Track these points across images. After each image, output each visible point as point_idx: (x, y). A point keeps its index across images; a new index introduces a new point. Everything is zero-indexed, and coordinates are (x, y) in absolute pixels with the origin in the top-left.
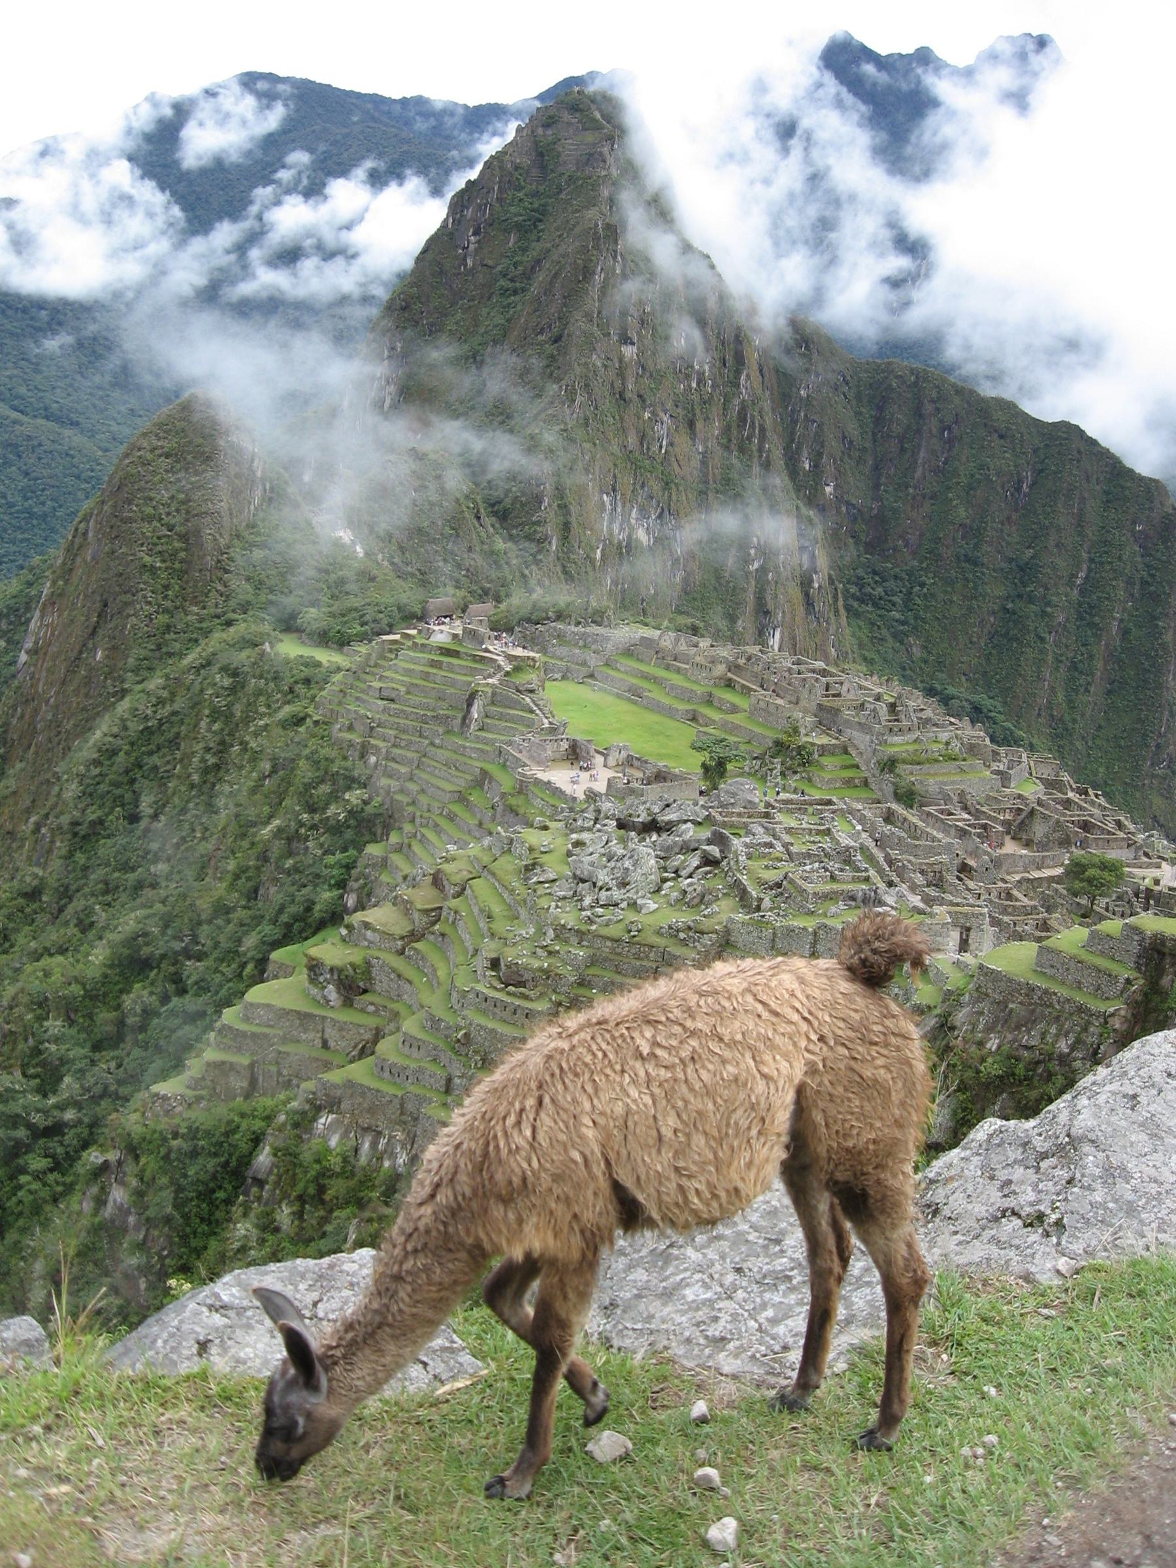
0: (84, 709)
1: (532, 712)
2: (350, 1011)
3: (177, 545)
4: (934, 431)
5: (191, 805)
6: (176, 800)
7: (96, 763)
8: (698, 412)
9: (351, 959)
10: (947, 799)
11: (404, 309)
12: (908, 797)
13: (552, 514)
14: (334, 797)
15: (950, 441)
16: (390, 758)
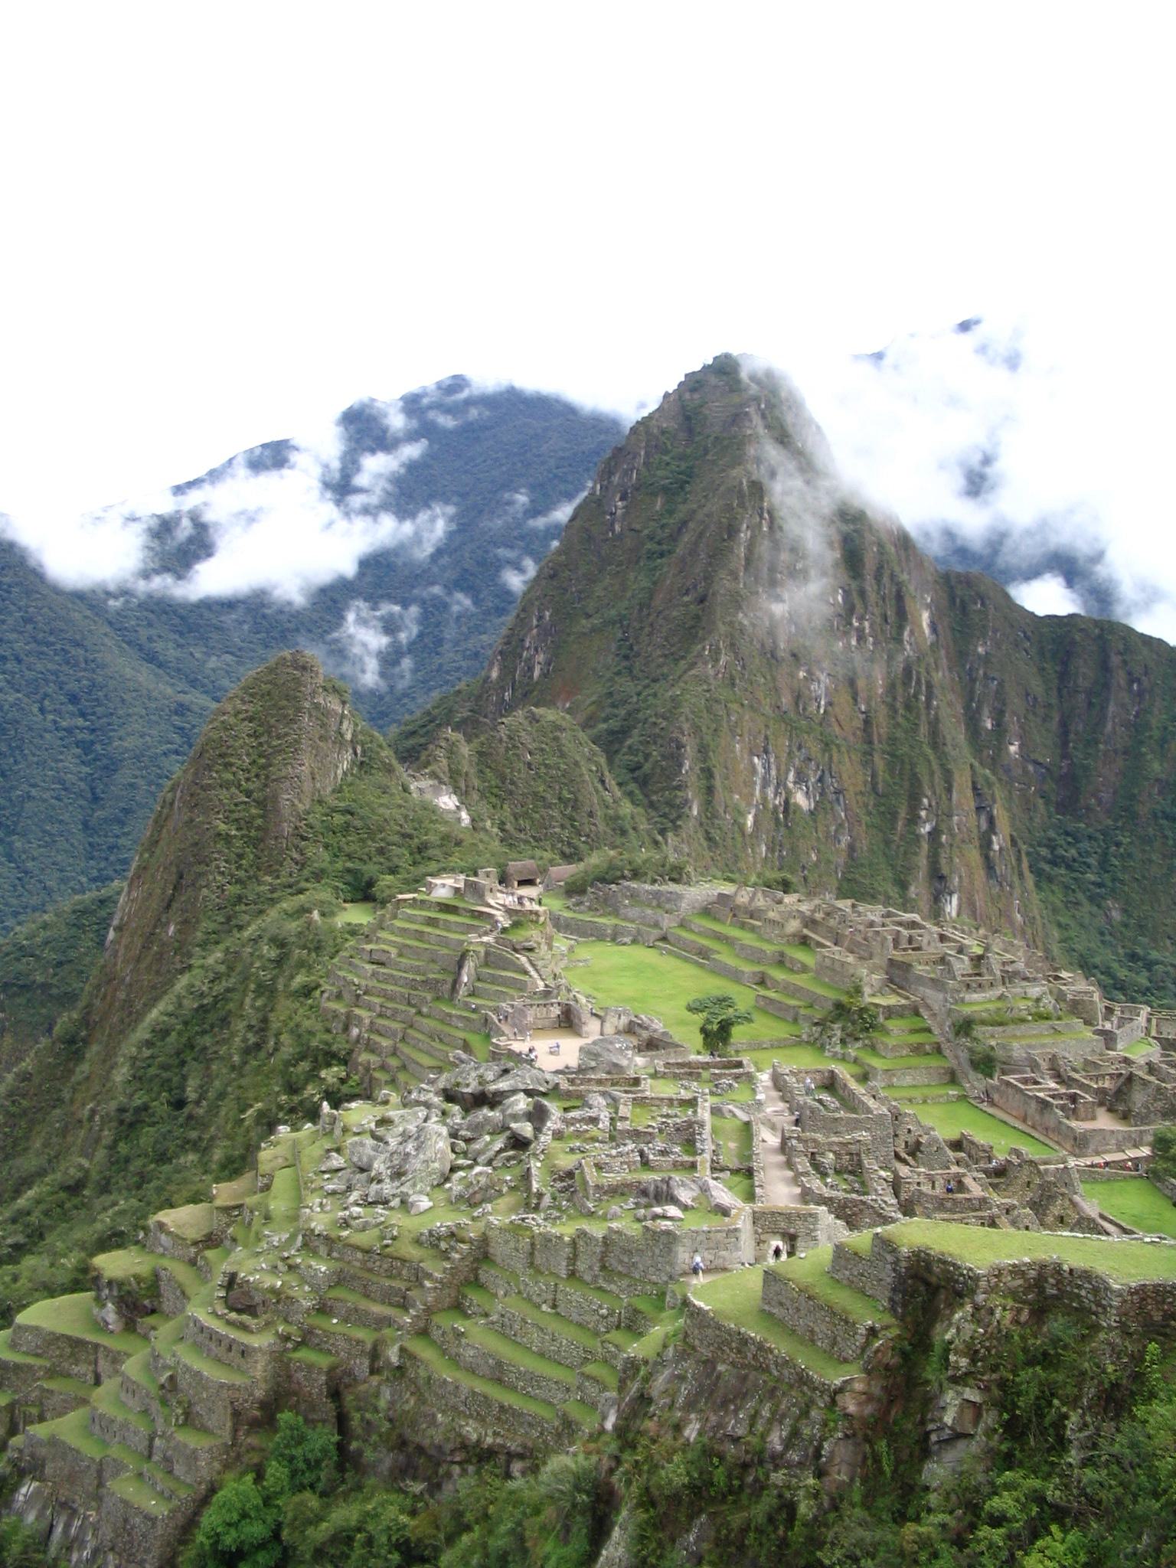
0: (154, 987)
1: (526, 973)
2: (132, 1337)
3: (254, 811)
4: (1122, 682)
6: (217, 1083)
7: (149, 1044)
9: (138, 1270)
10: (1034, 1066)
11: (552, 577)
12: (985, 1064)
13: (694, 778)
14: (312, 1076)
15: (1140, 694)
16: (373, 1028)
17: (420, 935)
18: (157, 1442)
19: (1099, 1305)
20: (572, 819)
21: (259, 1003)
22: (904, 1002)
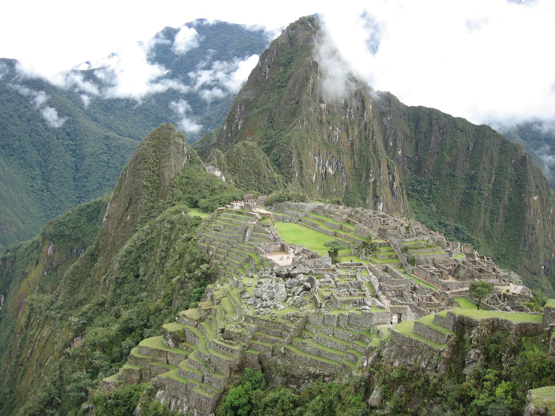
0: (123, 237)
2: (177, 349)
3: (156, 178)
4: (437, 130)
5: (156, 271)
6: (151, 269)
7: (125, 256)
8: (349, 126)
9: (178, 329)
10: (428, 262)
12: (412, 261)
13: (296, 164)
14: (197, 267)
15: (443, 133)
17: (230, 222)
18: (205, 378)
19: (509, 328)
20: (258, 179)
21: (165, 243)
22: (385, 242)
